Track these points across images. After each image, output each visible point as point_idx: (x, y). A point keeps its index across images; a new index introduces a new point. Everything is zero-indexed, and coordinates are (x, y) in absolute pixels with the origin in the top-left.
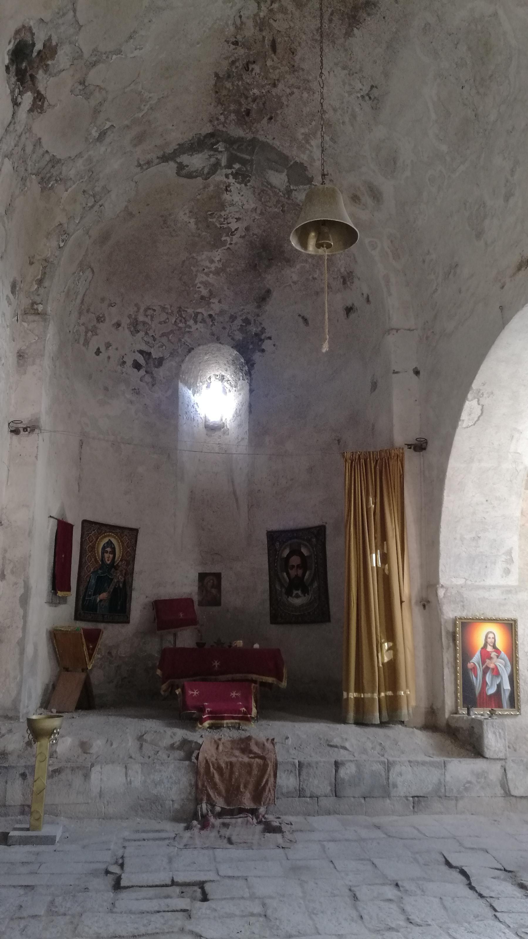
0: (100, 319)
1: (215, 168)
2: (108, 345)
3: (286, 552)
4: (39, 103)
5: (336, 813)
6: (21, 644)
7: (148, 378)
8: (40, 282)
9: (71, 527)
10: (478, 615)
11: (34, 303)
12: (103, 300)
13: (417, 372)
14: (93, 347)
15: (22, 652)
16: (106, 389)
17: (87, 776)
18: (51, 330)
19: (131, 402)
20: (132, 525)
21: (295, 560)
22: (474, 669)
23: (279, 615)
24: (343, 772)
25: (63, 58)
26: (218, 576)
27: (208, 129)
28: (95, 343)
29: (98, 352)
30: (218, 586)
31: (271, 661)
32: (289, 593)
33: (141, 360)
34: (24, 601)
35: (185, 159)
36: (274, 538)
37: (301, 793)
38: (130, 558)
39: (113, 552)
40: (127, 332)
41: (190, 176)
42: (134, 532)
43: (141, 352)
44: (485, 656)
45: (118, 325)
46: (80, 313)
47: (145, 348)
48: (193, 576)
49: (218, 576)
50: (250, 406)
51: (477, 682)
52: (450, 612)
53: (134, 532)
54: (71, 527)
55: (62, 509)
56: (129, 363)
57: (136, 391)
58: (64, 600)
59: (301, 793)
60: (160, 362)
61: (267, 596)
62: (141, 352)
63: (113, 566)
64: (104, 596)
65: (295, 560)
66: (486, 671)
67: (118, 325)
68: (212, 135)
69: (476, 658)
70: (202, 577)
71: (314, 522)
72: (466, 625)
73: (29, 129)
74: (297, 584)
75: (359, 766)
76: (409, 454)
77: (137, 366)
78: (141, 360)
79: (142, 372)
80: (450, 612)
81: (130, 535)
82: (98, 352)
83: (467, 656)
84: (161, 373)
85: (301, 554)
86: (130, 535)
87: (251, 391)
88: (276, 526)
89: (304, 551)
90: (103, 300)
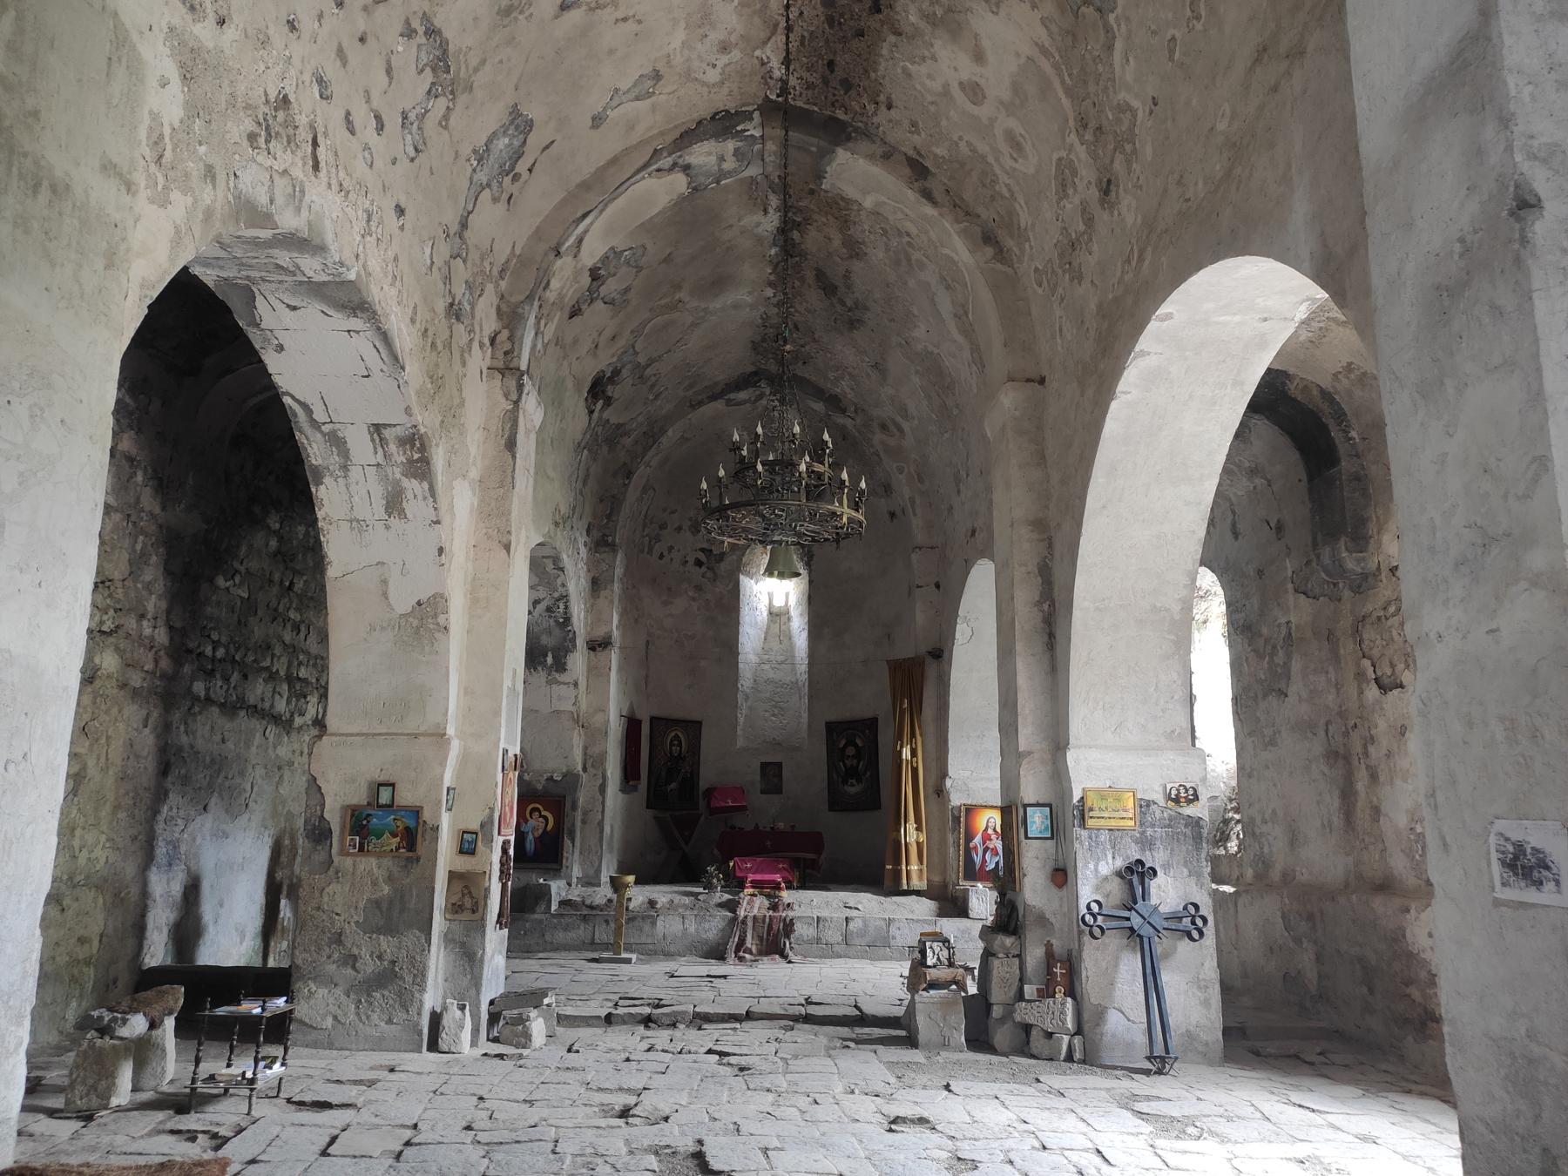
0: (663, 527)
1: (761, 396)
2: (671, 549)
3: (843, 742)
4: (608, 401)
5: (846, 956)
6: (601, 824)
7: (709, 574)
8: (609, 517)
9: (640, 722)
10: (981, 802)
11: (604, 535)
12: (664, 510)
13: (938, 586)
14: (656, 554)
15: (602, 831)
16: (669, 589)
17: (654, 924)
18: (620, 557)
19: (694, 599)
20: (696, 716)
21: (851, 751)
22: (975, 848)
23: (837, 802)
24: (851, 925)
25: (625, 373)
26: (779, 765)
27: (752, 369)
28: (657, 548)
29: (661, 556)
30: (780, 775)
31: (814, 841)
32: (845, 782)
33: (702, 557)
34: (602, 789)
35: (732, 396)
36: (832, 728)
37: (818, 941)
38: (695, 749)
39: (680, 744)
40: (688, 534)
41: (739, 404)
42: (700, 723)
43: (702, 550)
44: (986, 838)
45: (679, 529)
46: (644, 526)
47: (705, 546)
48: (756, 765)
49: (779, 765)
50: (810, 597)
51: (978, 860)
52: (956, 800)
53: (700, 723)
54: (640, 722)
55: (631, 708)
56: (691, 560)
57: (698, 588)
58: (635, 788)
59: (818, 941)
60: (722, 556)
61: (825, 784)
62: (702, 550)
63: (680, 757)
64: (673, 785)
65: (851, 751)
66: (986, 850)
67: (679, 529)
68: (755, 373)
69: (978, 840)
70: (764, 766)
71: (868, 714)
72: (970, 810)
73: (600, 418)
74: (852, 773)
75: (865, 921)
76: (929, 660)
77: (699, 563)
78: (702, 557)
79: (704, 569)
80: (956, 800)
81: (693, 727)
82: (661, 556)
83: (969, 837)
84: (723, 567)
85: (856, 745)
86: (693, 727)
87: (810, 582)
88: (833, 717)
89: (858, 741)
90: (664, 510)
